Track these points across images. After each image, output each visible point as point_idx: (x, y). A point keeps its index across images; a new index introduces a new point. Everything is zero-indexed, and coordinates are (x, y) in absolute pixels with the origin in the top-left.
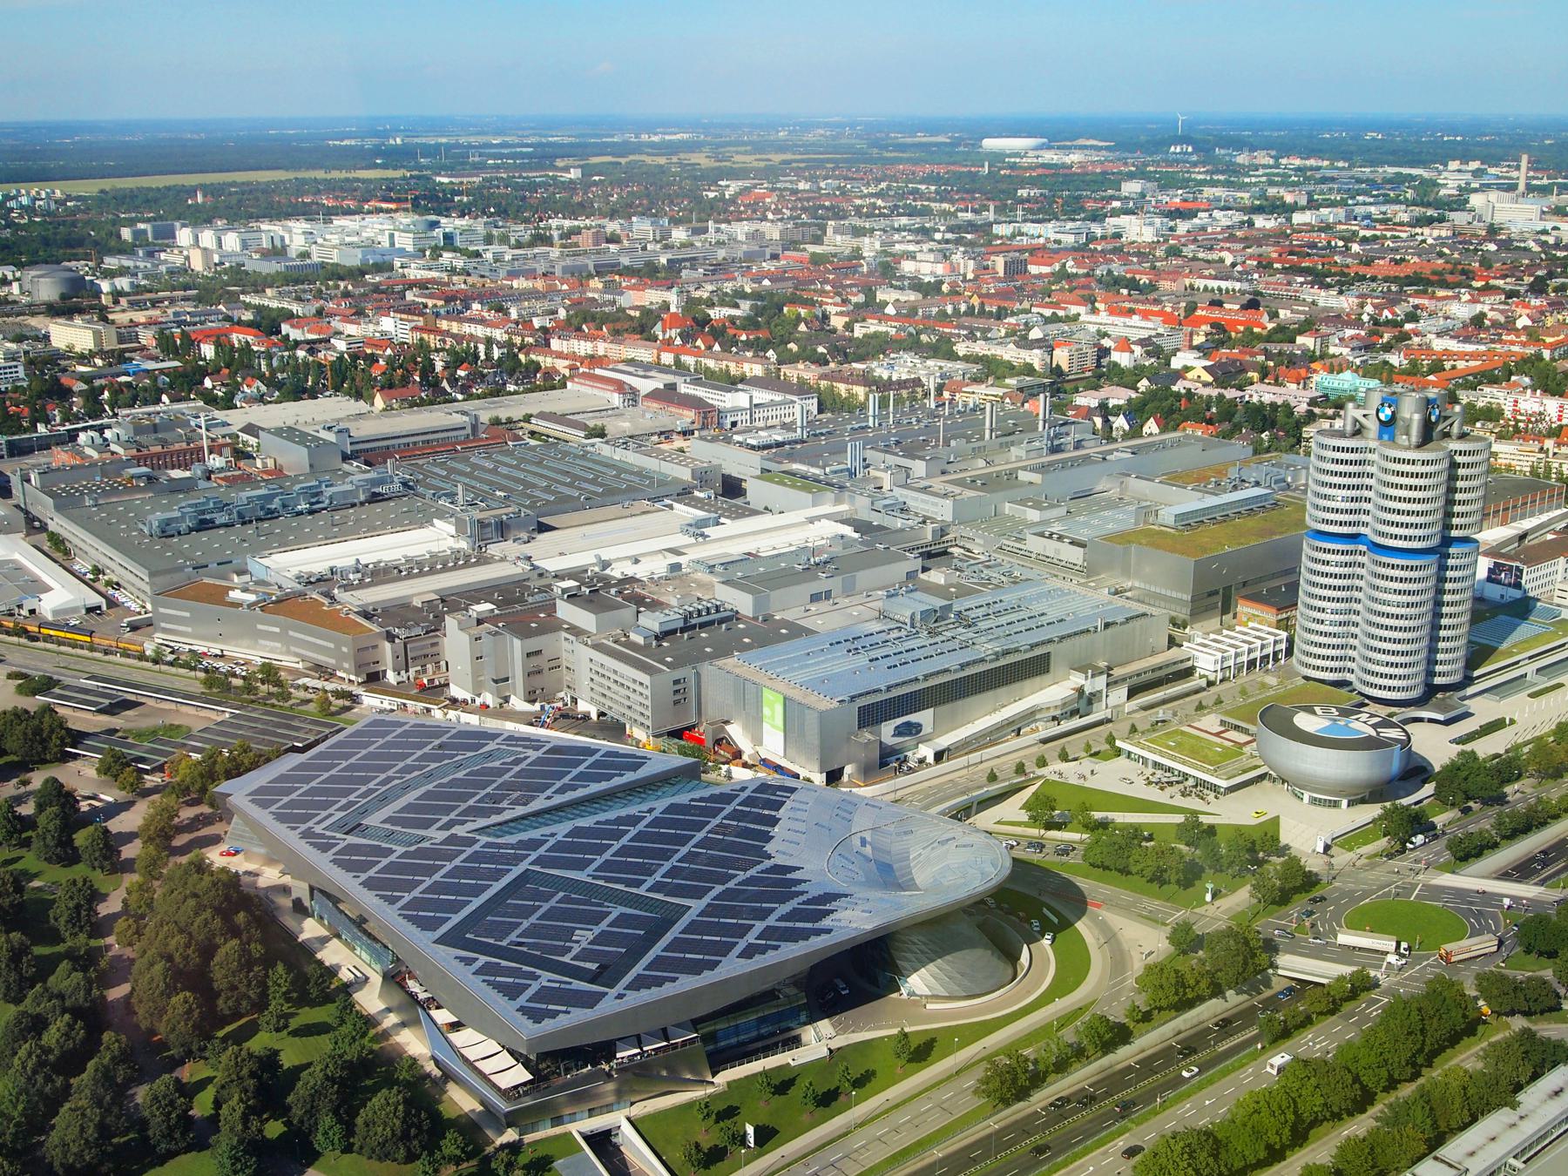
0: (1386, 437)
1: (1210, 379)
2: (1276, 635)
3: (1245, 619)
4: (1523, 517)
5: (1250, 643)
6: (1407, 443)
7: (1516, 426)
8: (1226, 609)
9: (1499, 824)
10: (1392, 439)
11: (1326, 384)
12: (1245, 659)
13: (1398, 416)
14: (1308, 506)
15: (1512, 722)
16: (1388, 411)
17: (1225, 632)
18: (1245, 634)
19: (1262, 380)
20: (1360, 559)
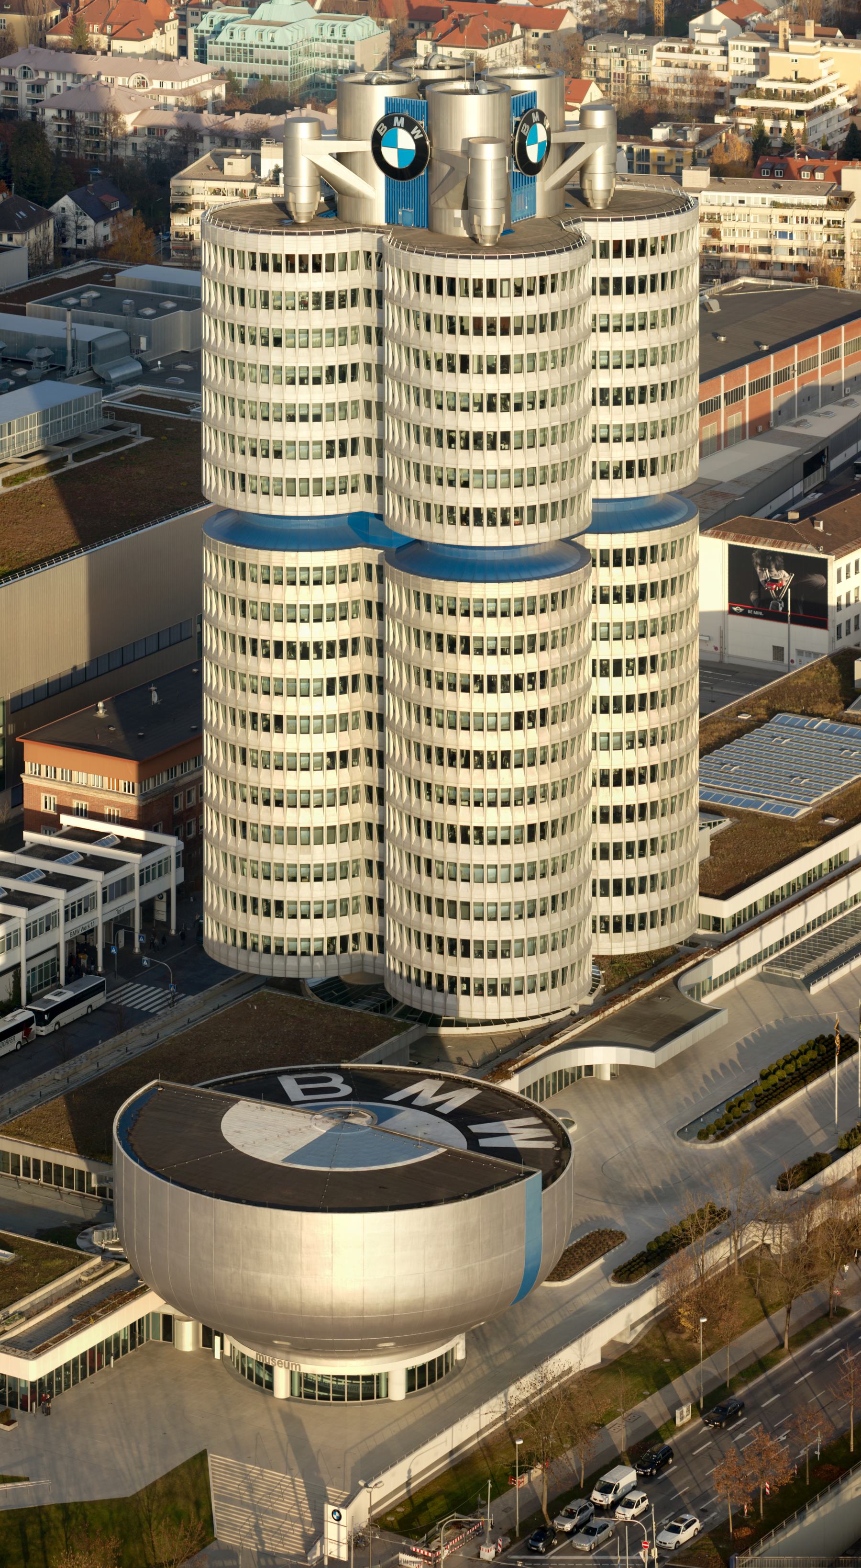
5: (68, 883)
12: (60, 935)
16: (406, 141)
18: (54, 854)
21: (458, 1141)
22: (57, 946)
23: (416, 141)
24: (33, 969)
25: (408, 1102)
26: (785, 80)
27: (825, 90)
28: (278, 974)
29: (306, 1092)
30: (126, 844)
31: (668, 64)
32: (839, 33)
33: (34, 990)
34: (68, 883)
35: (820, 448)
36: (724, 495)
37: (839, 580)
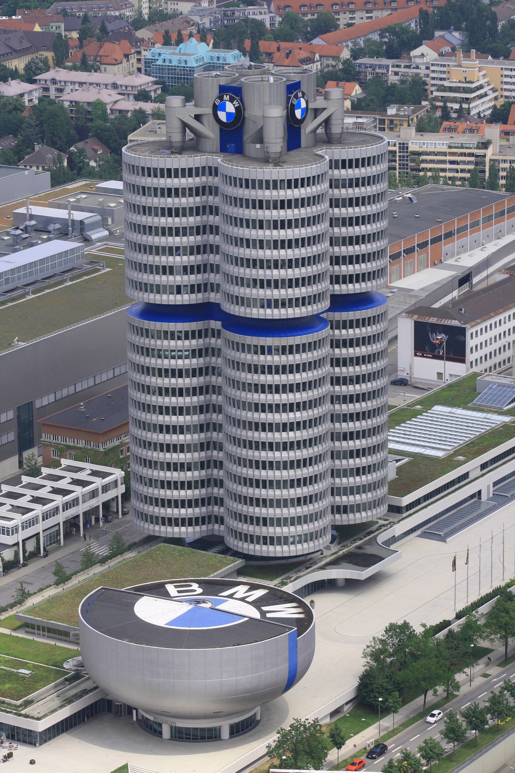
2: (104, 475)
4: (463, 249)
5: (64, 492)
11: (160, 62)
13: (247, 114)
16: (230, 108)
17: (26, 479)
21: (255, 614)
22: (59, 524)
23: (236, 108)
24: (47, 536)
25: (231, 596)
26: (460, 82)
27: (481, 87)
28: (170, 536)
29: (179, 592)
30: (94, 473)
31: (396, 74)
32: (490, 58)
33: (47, 546)
34: (64, 492)
35: (467, 272)
36: (416, 296)
37: (472, 338)
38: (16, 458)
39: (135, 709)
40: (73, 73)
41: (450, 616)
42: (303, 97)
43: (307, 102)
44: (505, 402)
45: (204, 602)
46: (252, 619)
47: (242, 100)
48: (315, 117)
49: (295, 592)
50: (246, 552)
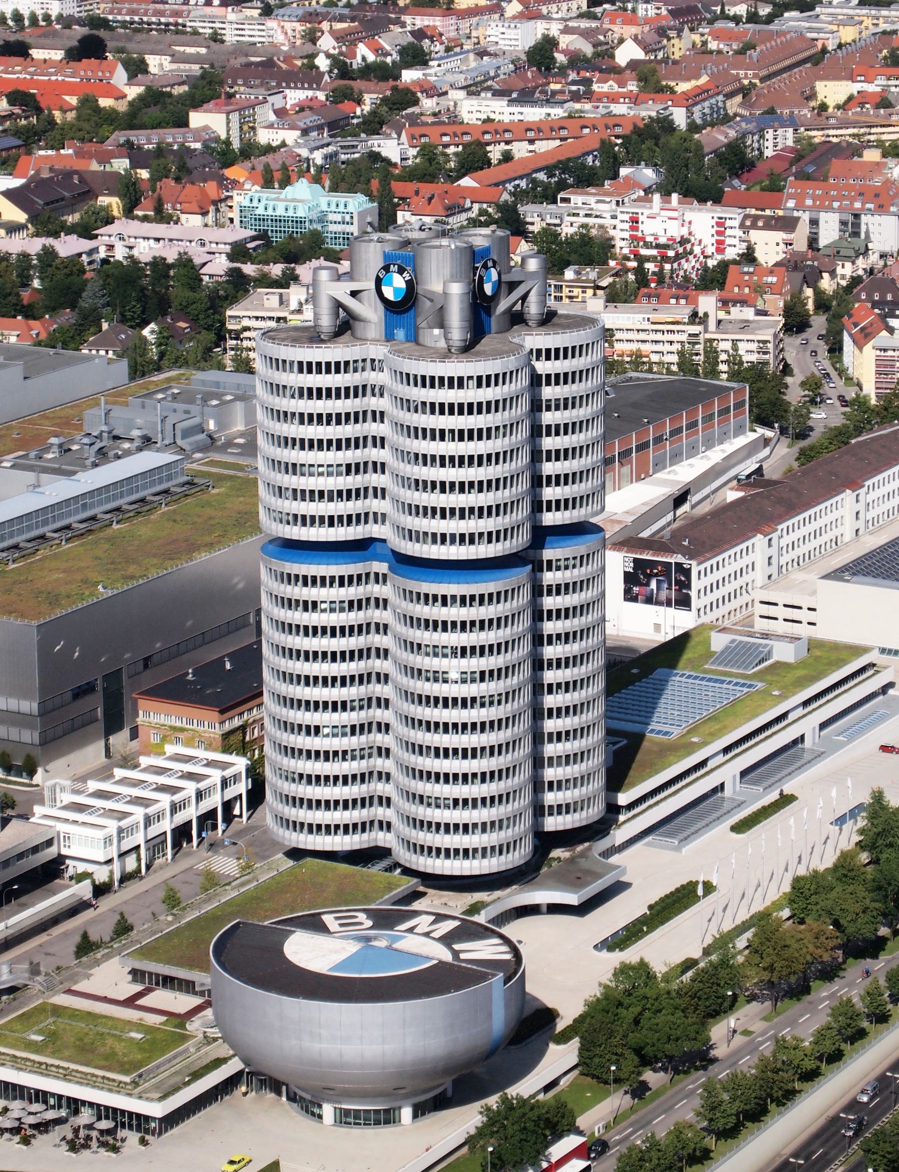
0: (400, 334)
1: (20, 216)
2: (224, 766)
3: (154, 739)
4: (676, 457)
5: (173, 790)
6: (442, 344)
7: (640, 272)
8: (113, 723)
9: (712, 1107)
10: (414, 338)
11: (257, 212)
13: (420, 289)
14: (262, 490)
15: (709, 888)
17: (119, 773)
18: (161, 771)
19: (128, 212)
20: (376, 590)
22: (165, 833)
25: (411, 930)
29: (341, 925)
30: (210, 764)
36: (619, 522)
38: (102, 743)
39: (284, 1084)
40: (146, 225)
41: (697, 954)
42: (494, 267)
43: (499, 274)
44: (751, 663)
45: (375, 938)
46: (441, 964)
47: (414, 270)
48: (510, 293)
49: (489, 922)
50: (422, 869)
